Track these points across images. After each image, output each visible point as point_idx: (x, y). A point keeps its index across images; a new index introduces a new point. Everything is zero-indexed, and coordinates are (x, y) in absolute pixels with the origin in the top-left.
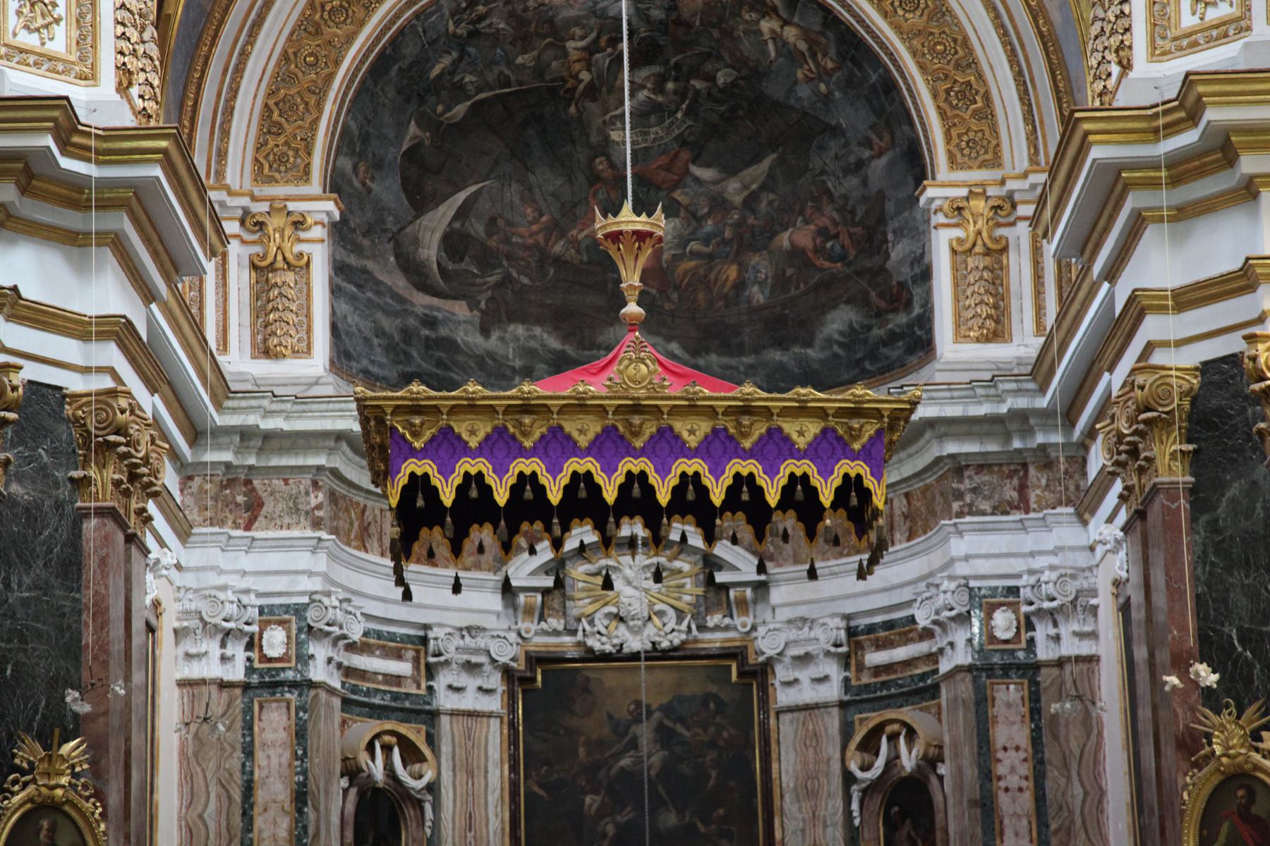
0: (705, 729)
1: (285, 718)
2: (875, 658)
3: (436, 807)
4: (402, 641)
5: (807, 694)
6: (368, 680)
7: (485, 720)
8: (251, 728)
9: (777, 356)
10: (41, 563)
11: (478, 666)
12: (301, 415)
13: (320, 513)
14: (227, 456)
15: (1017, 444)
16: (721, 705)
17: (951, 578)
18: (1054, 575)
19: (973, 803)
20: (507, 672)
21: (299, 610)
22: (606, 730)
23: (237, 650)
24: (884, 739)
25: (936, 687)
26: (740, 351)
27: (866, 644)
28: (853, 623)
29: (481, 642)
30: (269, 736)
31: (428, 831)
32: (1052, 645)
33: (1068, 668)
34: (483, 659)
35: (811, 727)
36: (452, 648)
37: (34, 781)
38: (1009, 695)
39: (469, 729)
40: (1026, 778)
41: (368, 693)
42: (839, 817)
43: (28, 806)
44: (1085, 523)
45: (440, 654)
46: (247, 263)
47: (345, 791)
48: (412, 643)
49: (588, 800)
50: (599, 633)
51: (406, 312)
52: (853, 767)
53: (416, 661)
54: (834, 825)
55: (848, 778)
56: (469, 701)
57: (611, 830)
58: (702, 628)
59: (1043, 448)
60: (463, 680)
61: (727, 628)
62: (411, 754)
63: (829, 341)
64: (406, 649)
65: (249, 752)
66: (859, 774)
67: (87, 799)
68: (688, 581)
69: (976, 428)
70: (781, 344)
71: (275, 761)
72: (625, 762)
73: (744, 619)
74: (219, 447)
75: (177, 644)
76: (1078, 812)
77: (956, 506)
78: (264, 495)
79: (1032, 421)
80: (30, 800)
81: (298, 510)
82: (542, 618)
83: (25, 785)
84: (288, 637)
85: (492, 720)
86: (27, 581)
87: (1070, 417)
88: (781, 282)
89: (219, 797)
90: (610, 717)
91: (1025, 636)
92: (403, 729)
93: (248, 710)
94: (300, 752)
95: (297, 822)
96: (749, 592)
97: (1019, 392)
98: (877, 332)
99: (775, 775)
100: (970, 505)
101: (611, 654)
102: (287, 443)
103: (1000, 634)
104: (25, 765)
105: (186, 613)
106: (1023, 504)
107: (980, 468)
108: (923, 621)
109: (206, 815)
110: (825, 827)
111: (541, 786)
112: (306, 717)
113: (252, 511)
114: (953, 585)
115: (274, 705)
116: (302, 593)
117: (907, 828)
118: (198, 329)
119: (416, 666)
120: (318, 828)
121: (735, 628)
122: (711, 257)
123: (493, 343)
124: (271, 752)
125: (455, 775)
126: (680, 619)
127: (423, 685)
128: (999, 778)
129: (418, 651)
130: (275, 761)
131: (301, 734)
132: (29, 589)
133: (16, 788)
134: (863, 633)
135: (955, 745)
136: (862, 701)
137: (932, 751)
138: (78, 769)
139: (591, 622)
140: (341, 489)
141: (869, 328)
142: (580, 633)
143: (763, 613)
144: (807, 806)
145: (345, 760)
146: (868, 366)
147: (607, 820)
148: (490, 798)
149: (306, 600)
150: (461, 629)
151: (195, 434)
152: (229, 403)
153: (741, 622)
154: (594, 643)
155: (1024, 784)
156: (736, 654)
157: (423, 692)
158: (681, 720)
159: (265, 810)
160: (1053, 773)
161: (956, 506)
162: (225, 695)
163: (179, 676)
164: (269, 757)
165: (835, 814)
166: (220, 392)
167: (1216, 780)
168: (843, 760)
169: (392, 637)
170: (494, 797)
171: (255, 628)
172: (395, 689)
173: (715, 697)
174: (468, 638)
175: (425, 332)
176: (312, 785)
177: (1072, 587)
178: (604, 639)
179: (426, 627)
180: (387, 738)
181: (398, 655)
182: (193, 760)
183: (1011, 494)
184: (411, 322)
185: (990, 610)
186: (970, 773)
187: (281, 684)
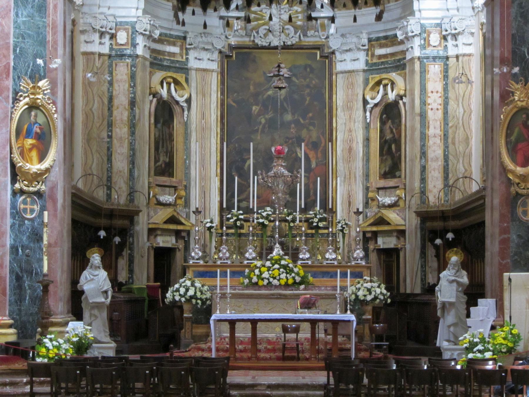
0: (305, 79)
1: (126, 70)
4: (176, 38)
5: (349, 66)
7: (210, 73)
10: (30, 6)
16: (312, 70)
20: (220, 52)
22: (262, 79)
23: (106, 40)
24: (382, 86)
25: (405, 65)
27: (376, 45)
29: (209, 39)
30: (119, 77)
31: (186, 119)
33: (460, 58)
34: (210, 47)
35: (350, 80)
37: (28, 96)
39: (204, 77)
40: (440, 105)
41: (161, 60)
42: (361, 118)
43: (27, 106)
45: (191, 44)
47: (151, 102)
48: (180, 39)
49: (254, 108)
50: (260, 37)
52: (368, 98)
54: (359, 122)
55: (365, 102)
57: (263, 121)
58: (305, 35)
64: (177, 42)
65: (111, 83)
67: (49, 104)
68: (300, 15)
71: (122, 88)
73: (323, 33)
76: (461, 119)
80: (27, 104)
83: (25, 97)
84: (128, 35)
85: (213, 73)
86: (25, 13)
89: (98, 102)
92: (175, 75)
93: (110, 66)
94: (132, 85)
95: (131, 114)
101: (265, 46)
104: (25, 89)
108: (400, 37)
109: (93, 109)
110: (355, 122)
111: (234, 102)
112: (135, 70)
115: (122, 64)
116: (134, 17)
117: (389, 123)
119: (181, 49)
120: (140, 116)
125: (197, 96)
126: (296, 33)
127: (184, 57)
128: (429, 104)
129: (182, 43)
131: (133, 77)
132: (26, 17)
133: (21, 98)
134: (374, 40)
136: (373, 70)
138: (45, 92)
142: (252, 37)
147: (262, 117)
148: (212, 106)
149: (135, 20)
150: (201, 34)
155: (439, 107)
157: (184, 60)
159: (118, 108)
160: (452, 103)
164: (119, 86)
165: (359, 117)
167: (515, 110)
168: (364, 95)
169: (171, 36)
170: (214, 106)
171: (113, 31)
172: (172, 59)
173: (310, 66)
174: (204, 38)
178: (263, 40)
181: (174, 44)
186: (417, 102)
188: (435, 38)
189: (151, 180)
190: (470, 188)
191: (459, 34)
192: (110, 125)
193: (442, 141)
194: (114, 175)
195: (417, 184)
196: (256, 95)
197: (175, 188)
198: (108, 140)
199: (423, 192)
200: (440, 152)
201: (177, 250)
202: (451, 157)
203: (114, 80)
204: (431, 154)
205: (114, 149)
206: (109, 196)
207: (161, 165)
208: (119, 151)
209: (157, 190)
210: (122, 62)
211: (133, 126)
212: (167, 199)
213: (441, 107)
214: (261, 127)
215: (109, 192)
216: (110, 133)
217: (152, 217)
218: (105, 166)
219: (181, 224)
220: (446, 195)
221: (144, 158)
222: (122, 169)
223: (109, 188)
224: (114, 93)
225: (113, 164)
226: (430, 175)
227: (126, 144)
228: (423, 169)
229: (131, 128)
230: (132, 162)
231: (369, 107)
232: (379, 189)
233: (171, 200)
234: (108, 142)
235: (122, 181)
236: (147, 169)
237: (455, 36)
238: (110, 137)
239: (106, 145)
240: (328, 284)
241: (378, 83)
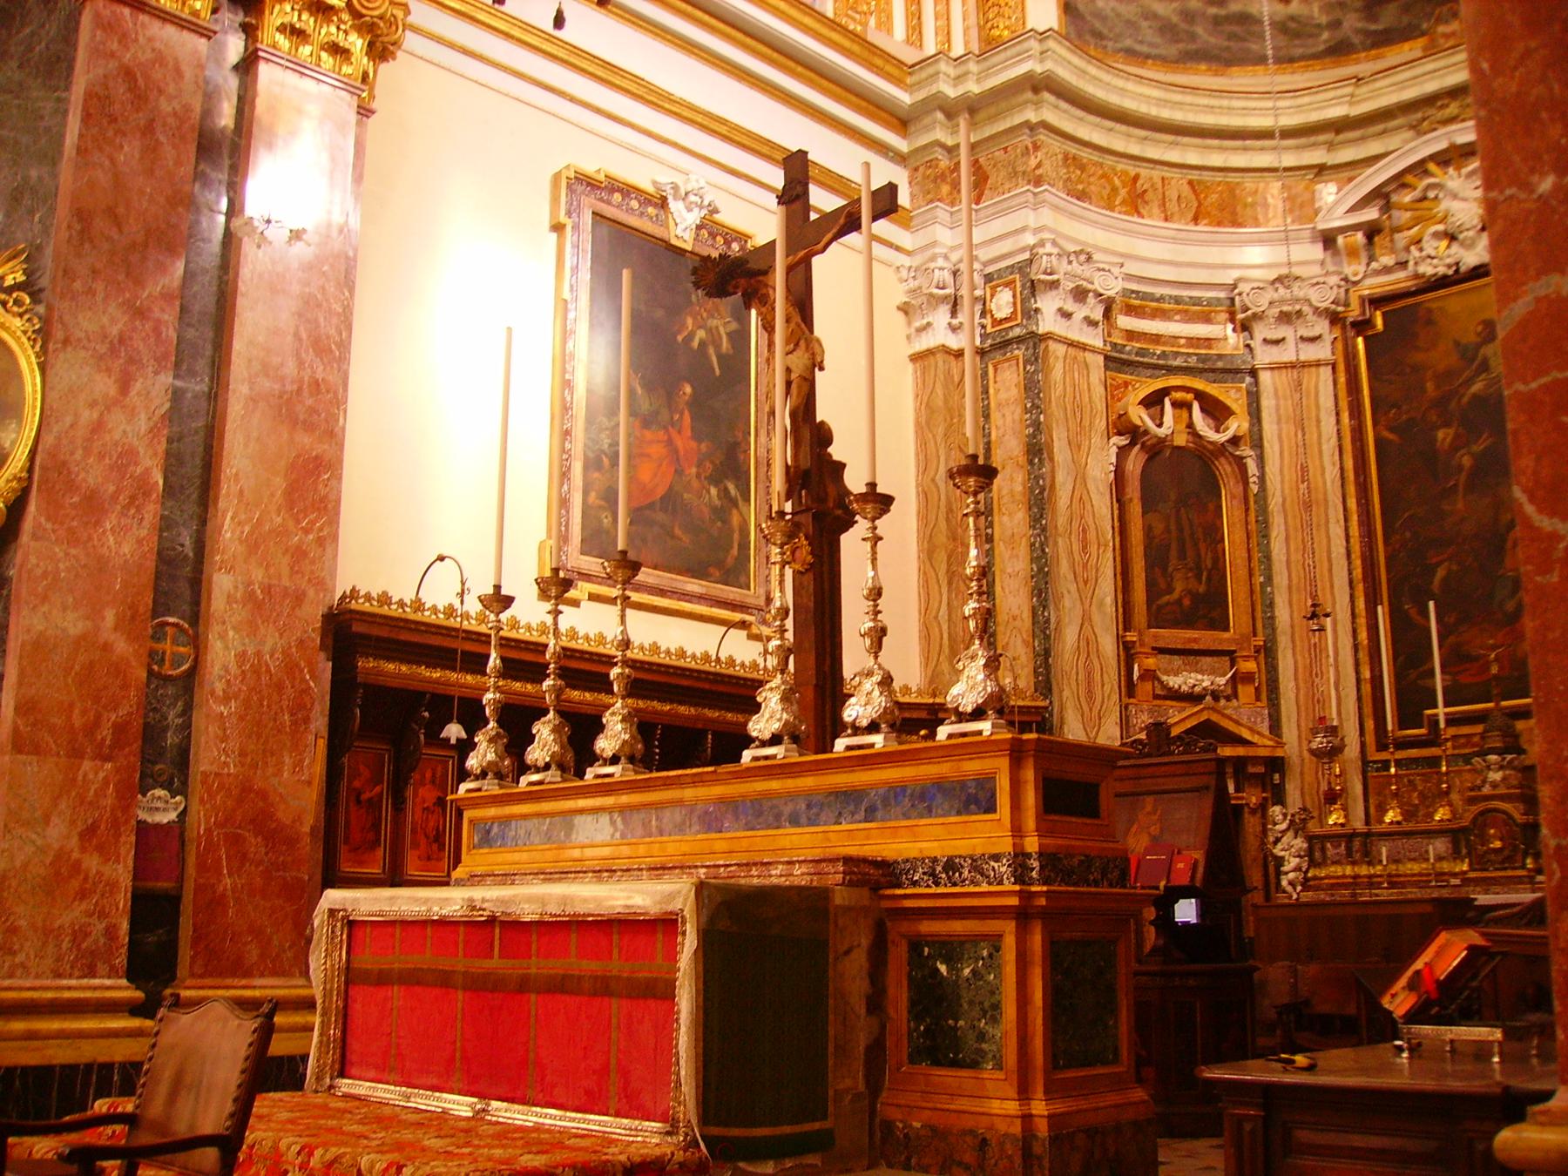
6: (1164, 344)
7: (1313, 369)
8: (987, 392)
11: (1299, 313)
20: (1335, 319)
21: (1023, 268)
36: (1260, 303)
41: (1164, 355)
49: (1440, 434)
50: (1429, 257)
56: (1287, 354)
57: (1467, 461)
62: (1217, 411)
71: (1009, 419)
72: (1477, 387)
74: (928, 129)
75: (909, 324)
81: (1016, 173)
82: (1371, 258)
84: (1014, 296)
85: (1322, 369)
90: (1457, 344)
92: (1199, 384)
95: (1029, 474)
101: (1445, 277)
111: (1391, 430)
115: (1006, 365)
116: (1023, 250)
130: (1009, 419)
147: (1463, 451)
148: (1324, 447)
149: (1026, 255)
150: (1273, 282)
151: (902, 122)
154: (1427, 269)
163: (911, 352)
169: (1197, 302)
170: (1329, 445)
174: (1282, 291)
178: (1435, 261)
181: (1207, 319)
182: (925, 428)
189: (1131, 636)
194: (1000, 629)
196: (1441, 403)
201: (1246, 809)
203: (993, 405)
207: (1179, 601)
208: (1009, 570)
209: (1151, 662)
210: (1008, 360)
212: (1192, 681)
214: (1463, 477)
222: (1017, 612)
224: (993, 437)
225: (997, 601)
227: (1023, 550)
235: (1019, 642)
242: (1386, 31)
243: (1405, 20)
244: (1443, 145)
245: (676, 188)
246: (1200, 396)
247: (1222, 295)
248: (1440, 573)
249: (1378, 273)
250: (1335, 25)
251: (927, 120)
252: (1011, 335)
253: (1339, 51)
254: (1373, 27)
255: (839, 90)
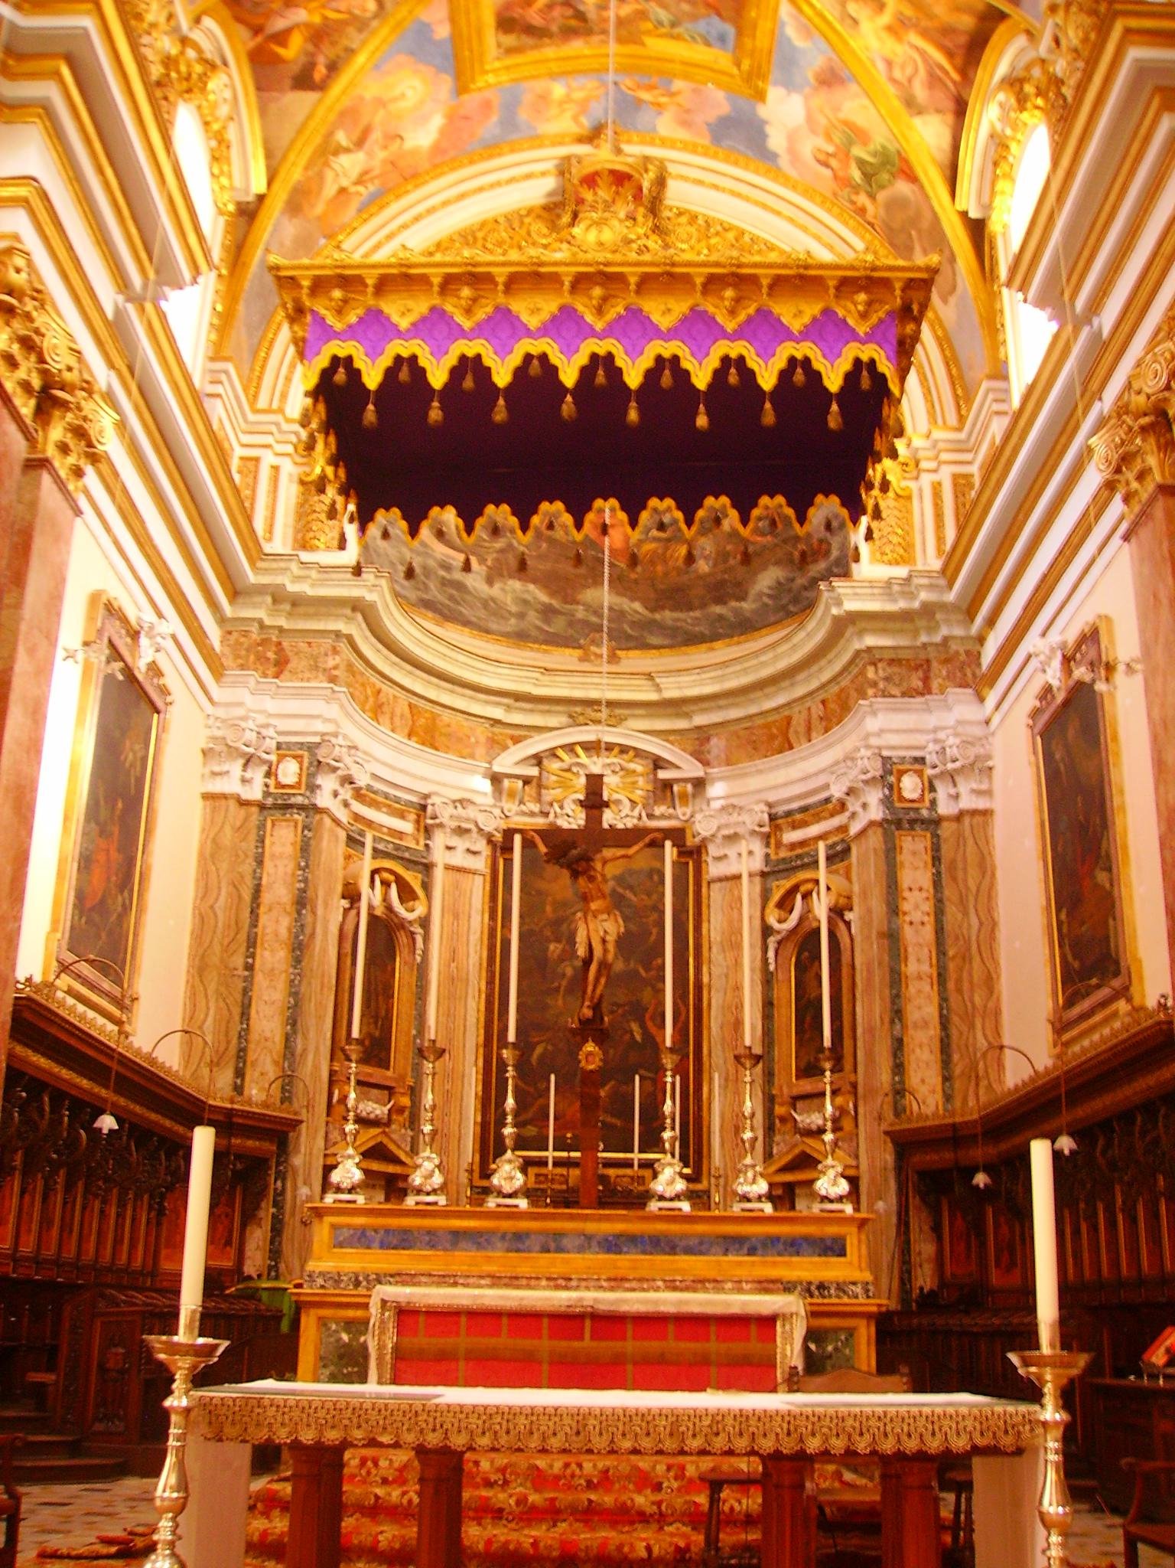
0: (649, 895)
1: (292, 835)
2: (791, 836)
3: (426, 938)
8: (263, 842)
9: (718, 609)
11: (468, 831)
12: (321, 583)
13: (335, 672)
14: (260, 613)
15: (924, 638)
17: (868, 747)
18: (957, 741)
19: (881, 935)
20: (490, 841)
21: (312, 748)
23: (258, 775)
24: (799, 897)
26: (691, 609)
28: (773, 811)
31: (419, 959)
32: (952, 803)
33: (967, 820)
34: (471, 826)
36: (446, 814)
38: (913, 848)
44: (982, 699)
46: (296, 479)
47: (346, 911)
49: (552, 947)
51: (427, 555)
52: (772, 921)
53: (418, 822)
55: (767, 931)
56: (458, 859)
58: (650, 816)
59: (946, 639)
60: (454, 841)
61: (670, 817)
62: (407, 894)
63: (760, 595)
65: (260, 862)
66: (776, 926)
69: (890, 625)
70: (721, 600)
71: (281, 869)
73: (684, 809)
74: (255, 606)
75: (205, 764)
76: (974, 938)
77: (870, 692)
78: (290, 654)
79: (938, 616)
87: (971, 613)
88: (722, 556)
89: (230, 895)
91: (928, 797)
93: (262, 827)
96: (689, 787)
97: (931, 587)
98: (801, 581)
99: (704, 931)
100: (883, 691)
102: (311, 610)
103: (907, 794)
105: (214, 738)
106: (926, 690)
107: (892, 662)
108: (837, 791)
109: (217, 906)
113: (281, 665)
114: (869, 753)
116: (315, 734)
118: (249, 519)
120: (314, 929)
121: (677, 818)
122: (668, 540)
123: (496, 591)
124: (278, 863)
126: (633, 809)
127: (422, 842)
128: (905, 913)
129: (419, 816)
130: (281, 869)
131: (305, 849)
135: (864, 894)
136: (779, 872)
137: (842, 901)
139: (561, 807)
140: (359, 665)
141: (793, 580)
142: (552, 815)
143: (699, 803)
144: (730, 955)
145: (347, 885)
146: (792, 608)
148: (472, 938)
149: (317, 739)
150: (454, 802)
151: (235, 593)
152: (260, 564)
153: (682, 812)
155: (926, 919)
156: (677, 835)
157: (421, 848)
158: (631, 888)
159: (270, 910)
160: (952, 911)
161: (870, 692)
162: (243, 812)
163: (204, 790)
166: (254, 553)
169: (397, 800)
171: (273, 758)
175: (442, 573)
176: (310, 893)
177: (972, 752)
179: (426, 796)
180: (386, 875)
181: (402, 816)
183: (917, 683)
184: (431, 563)
185: (901, 773)
186: (878, 906)
187: (291, 806)
188: (910, 786)
190: (1001, 1081)
191: (960, 771)
192: (252, 943)
193: (935, 987)
194: (252, 1046)
195: (885, 1077)
197: (390, 1090)
198: (247, 973)
199: (899, 1091)
200: (931, 1011)
202: (955, 1019)
203: (267, 854)
204: (913, 1014)
205: (254, 994)
206: (239, 1089)
208: (266, 998)
211: (299, 948)
212: (369, 1109)
213: (930, 920)
214: (564, 983)
215: (239, 1081)
216: (250, 960)
217: (335, 1144)
218: (236, 1027)
219: (397, 1161)
220: (948, 1098)
221: (321, 1018)
222: (268, 1034)
223: (240, 1073)
224: (264, 881)
225: (252, 1022)
226: (912, 1058)
227: (281, 984)
228: (898, 1045)
229: (293, 950)
230: (293, 1020)
231: (772, 942)
232: (795, 1099)
233: (378, 1112)
234: (245, 980)
235: (269, 1060)
236: (329, 1043)
237: (951, 777)
238: (250, 968)
239: (242, 985)
240: (742, 1273)
241: (794, 889)
242: (555, 634)
243: (570, 632)
244: (592, 737)
245: (152, 627)
246: (399, 880)
247: (414, 799)
248: (539, 1050)
249: (524, 813)
250: (521, 616)
251: (258, 599)
252: (293, 800)
253: (521, 637)
254: (546, 628)
255: (216, 558)
